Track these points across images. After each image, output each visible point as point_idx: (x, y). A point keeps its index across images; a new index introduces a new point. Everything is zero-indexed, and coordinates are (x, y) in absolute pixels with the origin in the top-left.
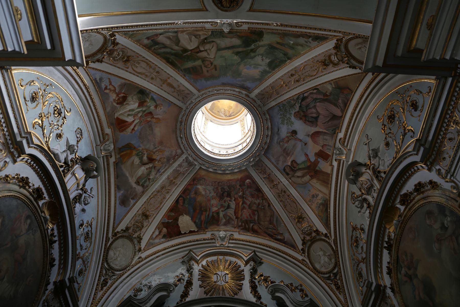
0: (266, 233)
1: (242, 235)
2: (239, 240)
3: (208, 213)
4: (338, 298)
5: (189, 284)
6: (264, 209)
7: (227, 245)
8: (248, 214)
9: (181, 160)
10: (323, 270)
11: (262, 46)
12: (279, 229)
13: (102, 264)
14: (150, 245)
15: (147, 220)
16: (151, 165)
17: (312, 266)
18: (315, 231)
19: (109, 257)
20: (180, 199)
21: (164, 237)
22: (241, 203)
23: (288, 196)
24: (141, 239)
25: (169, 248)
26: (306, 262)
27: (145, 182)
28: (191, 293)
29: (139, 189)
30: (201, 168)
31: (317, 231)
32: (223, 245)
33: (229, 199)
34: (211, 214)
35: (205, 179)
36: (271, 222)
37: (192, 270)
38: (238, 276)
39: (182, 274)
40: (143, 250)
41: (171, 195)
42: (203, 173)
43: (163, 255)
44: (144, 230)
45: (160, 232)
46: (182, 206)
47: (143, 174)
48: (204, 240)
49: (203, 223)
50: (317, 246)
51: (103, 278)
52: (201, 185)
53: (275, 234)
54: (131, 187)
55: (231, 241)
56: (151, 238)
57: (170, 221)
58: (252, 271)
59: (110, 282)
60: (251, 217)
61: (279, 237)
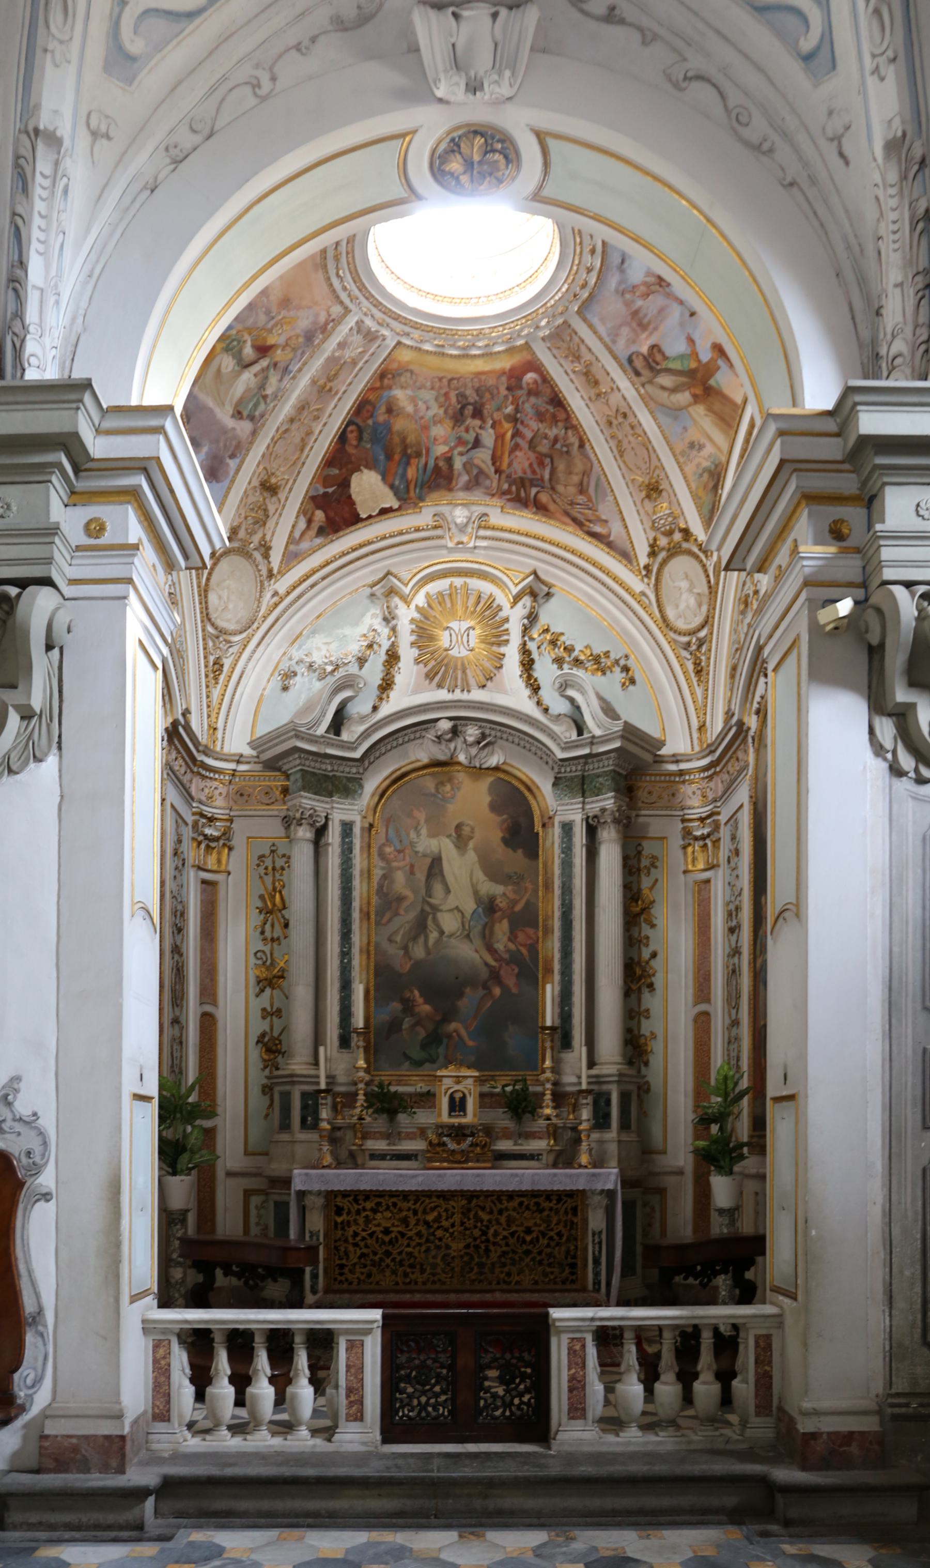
0: (567, 514)
1: (508, 517)
2: (502, 529)
3: (423, 460)
4: (692, 694)
5: (393, 657)
6: (567, 452)
7: (471, 545)
8: (526, 464)
9: (343, 330)
10: (681, 625)
12: (601, 507)
13: (203, 630)
14: (291, 558)
15: (274, 499)
16: (264, 363)
17: (660, 611)
18: (681, 530)
19: (211, 610)
20: (350, 428)
21: (321, 532)
22: (509, 434)
23: (632, 428)
24: (269, 548)
25: (336, 559)
26: (647, 597)
27: (256, 406)
28: (398, 679)
29: (245, 427)
30: (399, 343)
31: (686, 533)
32: (462, 543)
33: (477, 422)
34: (431, 463)
35: (412, 372)
36: (582, 489)
37: (394, 622)
38: (496, 637)
39: (374, 630)
40: (279, 572)
41: (325, 424)
42: (405, 356)
43: (323, 578)
44: (271, 523)
45: (309, 522)
46: (356, 447)
47: (248, 390)
48: (417, 530)
49: (412, 486)
50: (680, 565)
51: (212, 659)
52: (402, 387)
53: (589, 521)
54: (224, 430)
55: (482, 533)
56: (291, 540)
57: (330, 490)
58: (526, 621)
59: (227, 663)
60: (534, 472)
61: (597, 529)
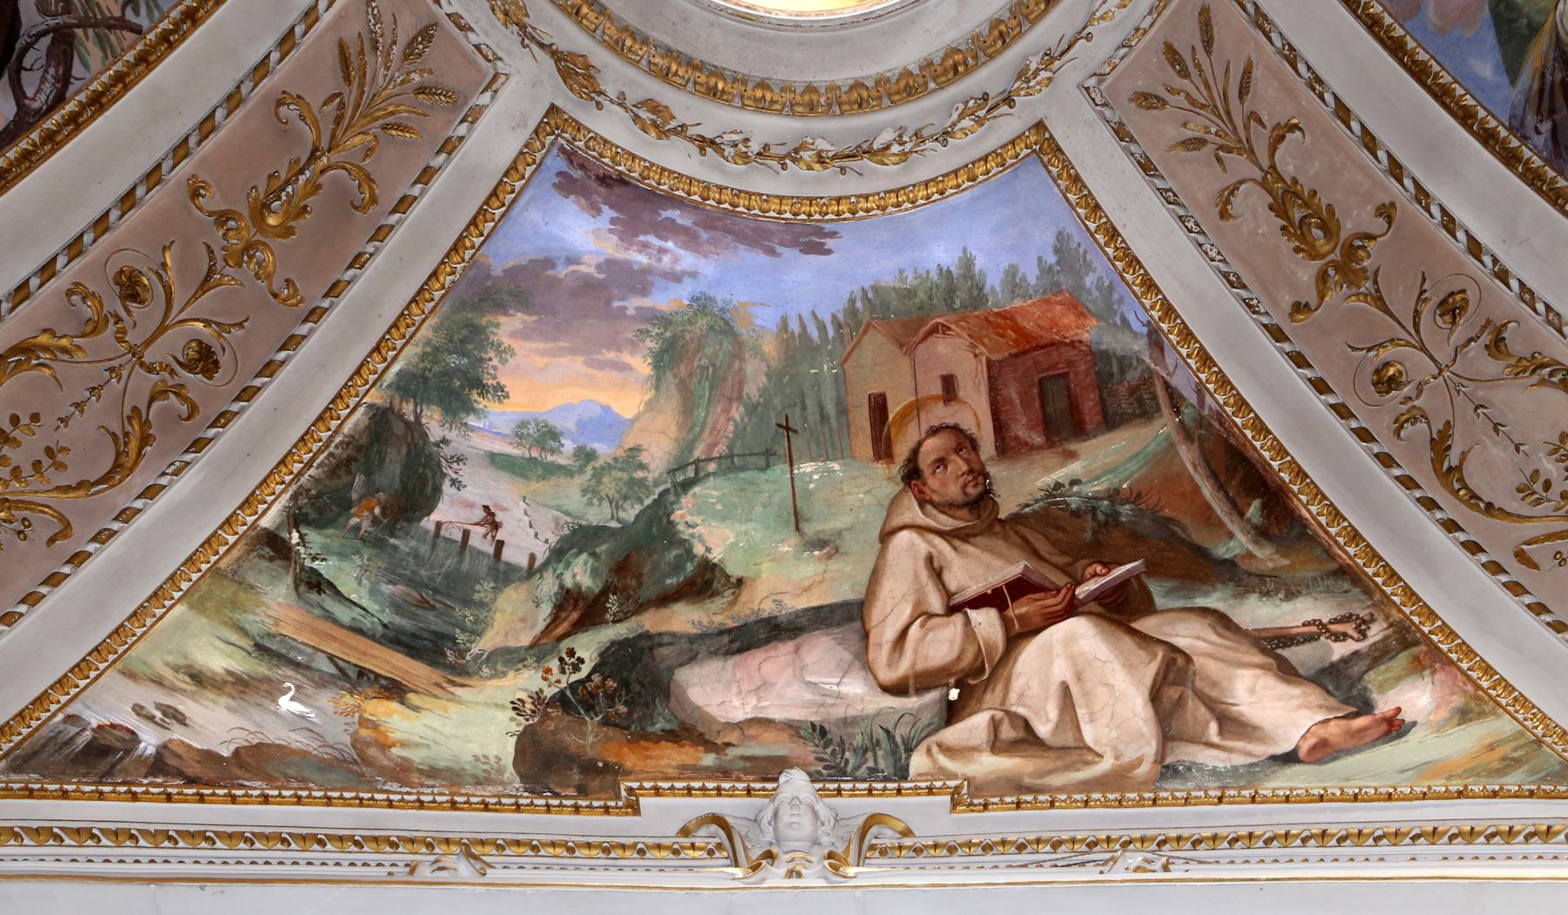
11: (508, 658)
